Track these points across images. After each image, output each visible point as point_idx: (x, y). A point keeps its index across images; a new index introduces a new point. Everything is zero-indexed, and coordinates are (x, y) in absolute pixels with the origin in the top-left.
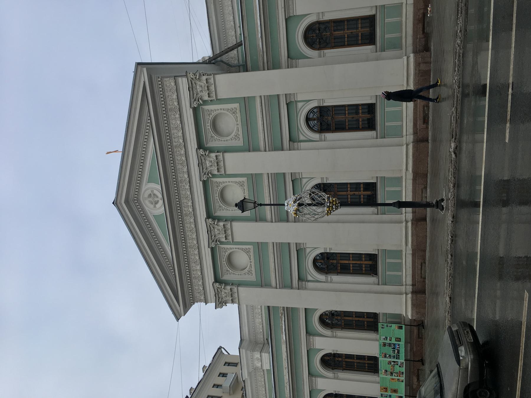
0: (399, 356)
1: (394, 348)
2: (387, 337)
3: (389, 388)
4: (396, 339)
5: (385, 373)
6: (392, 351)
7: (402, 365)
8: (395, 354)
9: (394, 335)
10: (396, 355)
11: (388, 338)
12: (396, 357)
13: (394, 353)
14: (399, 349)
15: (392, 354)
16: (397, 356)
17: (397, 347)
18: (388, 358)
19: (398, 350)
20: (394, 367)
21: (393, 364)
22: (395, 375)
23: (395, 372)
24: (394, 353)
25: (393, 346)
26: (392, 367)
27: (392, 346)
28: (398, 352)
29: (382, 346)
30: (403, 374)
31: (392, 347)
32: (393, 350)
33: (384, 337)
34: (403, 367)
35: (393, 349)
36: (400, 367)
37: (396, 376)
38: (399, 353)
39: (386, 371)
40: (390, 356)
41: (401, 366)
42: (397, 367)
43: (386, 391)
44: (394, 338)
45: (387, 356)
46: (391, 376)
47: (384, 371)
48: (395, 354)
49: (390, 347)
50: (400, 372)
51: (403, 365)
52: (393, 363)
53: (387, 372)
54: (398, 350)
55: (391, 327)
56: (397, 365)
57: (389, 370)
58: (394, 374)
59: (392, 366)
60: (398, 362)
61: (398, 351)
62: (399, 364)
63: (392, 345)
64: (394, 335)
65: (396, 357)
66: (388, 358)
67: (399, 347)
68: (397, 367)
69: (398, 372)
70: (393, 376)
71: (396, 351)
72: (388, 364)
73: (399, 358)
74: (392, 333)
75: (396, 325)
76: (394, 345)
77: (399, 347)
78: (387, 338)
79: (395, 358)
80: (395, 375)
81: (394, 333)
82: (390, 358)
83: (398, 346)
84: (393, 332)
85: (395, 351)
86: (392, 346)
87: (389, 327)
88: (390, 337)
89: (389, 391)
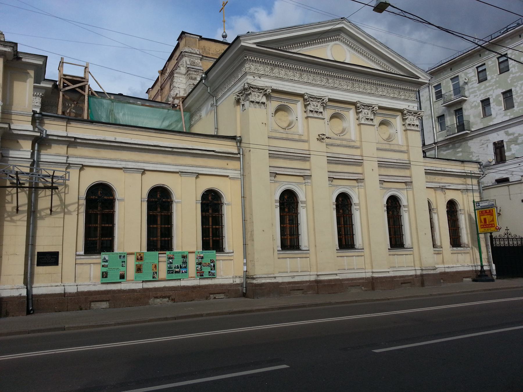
0: (172, 273)
1: (181, 267)
2: (107, 262)
3: (142, 262)
4: (105, 272)
5: (199, 257)
6: (178, 265)
7: (212, 275)
8: (174, 269)
9: (110, 269)
10: (172, 270)
11: (106, 264)
12: (170, 270)
13: (175, 268)
14: (181, 272)
15: (173, 265)
16: (172, 270)
17: (183, 271)
18: (168, 261)
19: (180, 271)
20: (208, 266)
21: (211, 265)
22: (198, 267)
23: (203, 267)
24: (175, 268)
25: (183, 266)
26: (207, 263)
27: (184, 265)
28: (176, 272)
29: (182, 254)
30: (200, 276)
31: (183, 265)
32: (179, 266)
33: (107, 259)
34: (209, 275)
35: (180, 266)
36: (209, 272)
37: (198, 268)
38: (175, 273)
39: (202, 258)
40: (171, 263)
41: (211, 274)
42: (209, 269)
43: (138, 259)
44: (107, 270)
45: (171, 260)
46: (197, 263)
47: (202, 255)
48: (174, 269)
49: (182, 263)
50: (203, 272)
51: (212, 276)
52: (213, 265)
53: (201, 259)
54: (180, 271)
55: (123, 266)
56: (211, 270)
57: (204, 261)
58: (199, 266)
59: (208, 264)
60: (215, 270)
61: (178, 271)
62: (213, 271)
63: (185, 265)
64: (110, 269)
65: (170, 270)
66: (168, 261)
67: (183, 273)
68: (209, 269)
69: (203, 271)
70: (197, 266)
71: (177, 270)
72: (211, 260)
73: (170, 273)
74: (115, 268)
75: (125, 271)
76: (184, 267)
77: (183, 273)
78: (107, 261)
79: (169, 269)
80: (198, 267)
81: (111, 270)
82: (168, 264)
83: (184, 272)
84: (115, 268)
85: (178, 268)
86: (184, 265)
87: (121, 264)
88: (107, 265)
89: (138, 262)
